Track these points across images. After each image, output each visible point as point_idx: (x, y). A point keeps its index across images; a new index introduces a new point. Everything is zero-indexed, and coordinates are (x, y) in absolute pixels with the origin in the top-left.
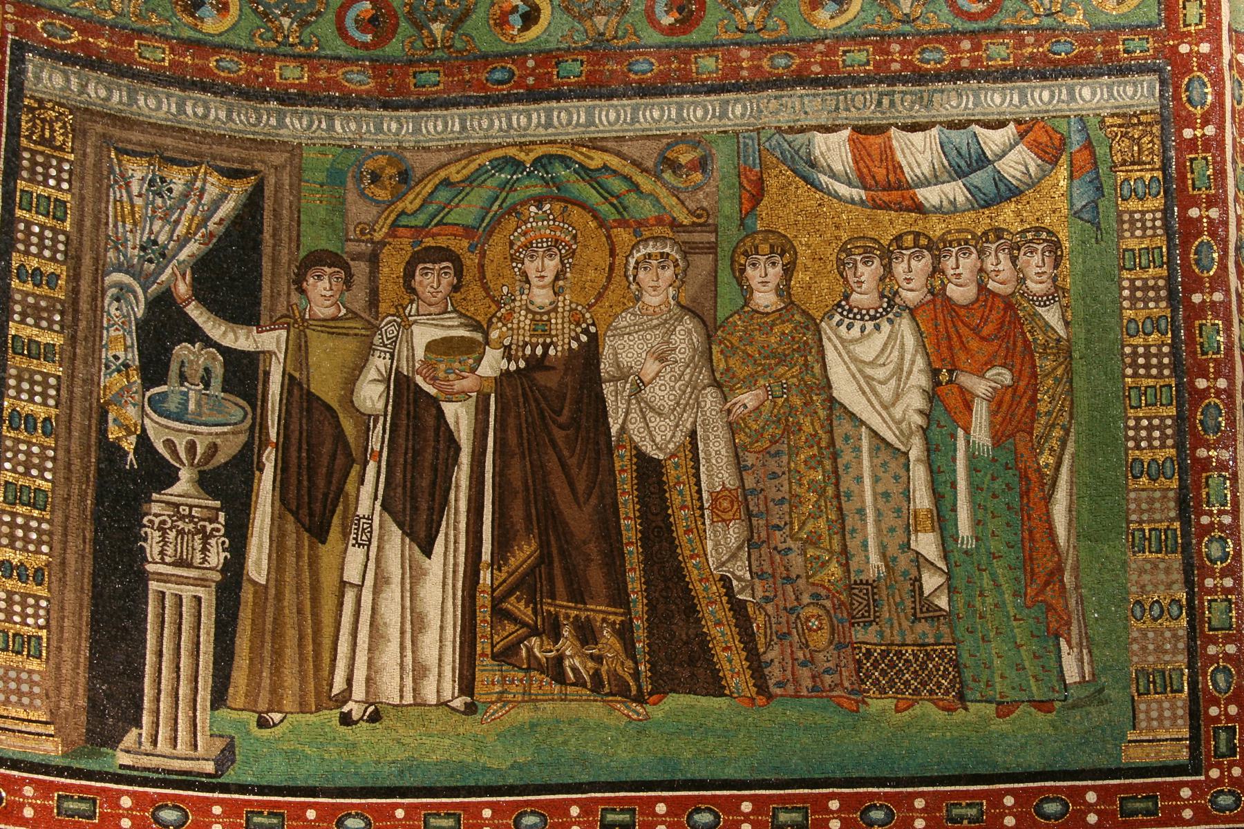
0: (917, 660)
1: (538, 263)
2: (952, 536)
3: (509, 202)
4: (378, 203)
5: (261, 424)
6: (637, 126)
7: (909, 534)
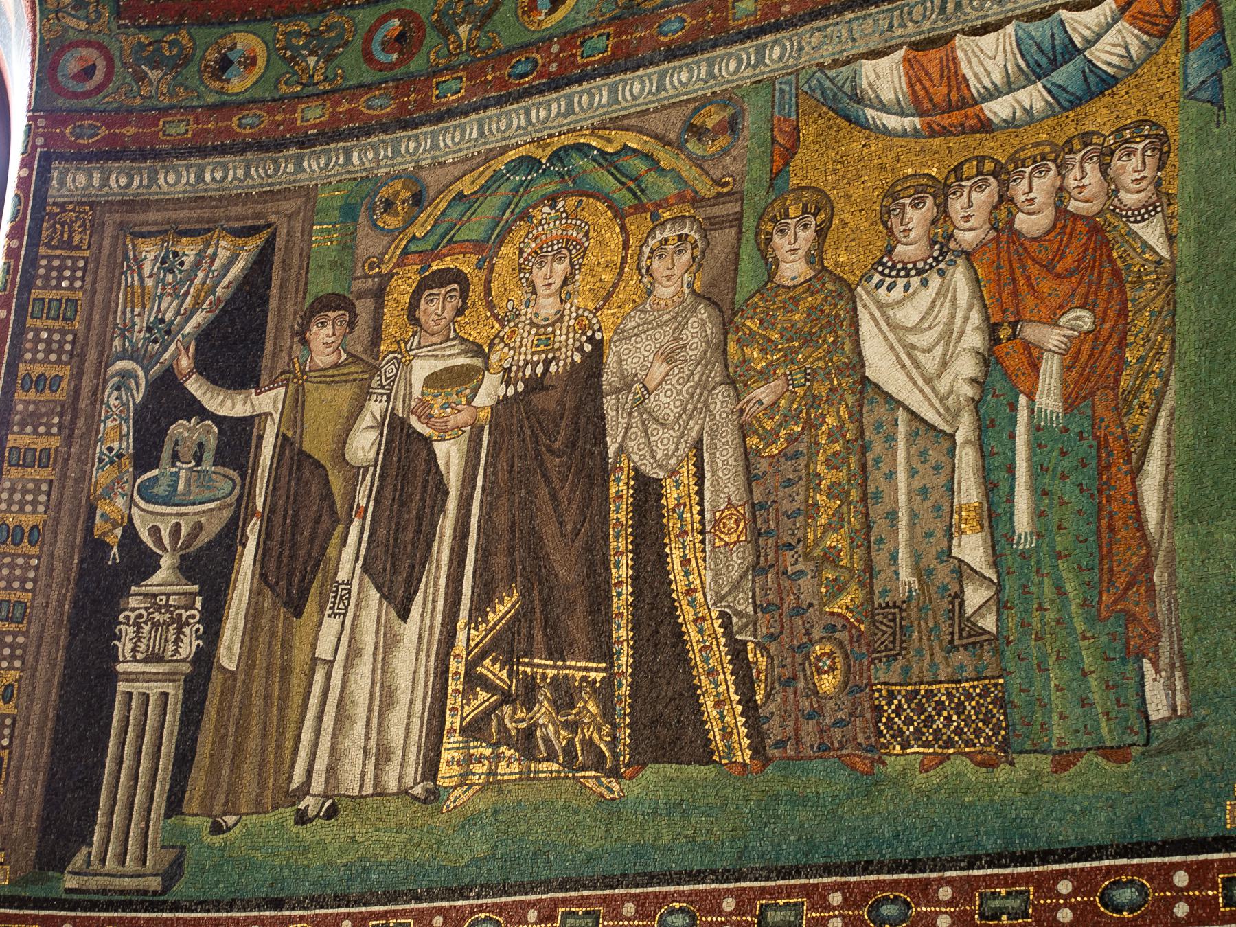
0: (951, 701)
1: (546, 269)
2: (1005, 535)
3: (522, 204)
4: (390, 231)
5: (249, 493)
6: (663, 94)
7: (951, 539)
